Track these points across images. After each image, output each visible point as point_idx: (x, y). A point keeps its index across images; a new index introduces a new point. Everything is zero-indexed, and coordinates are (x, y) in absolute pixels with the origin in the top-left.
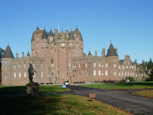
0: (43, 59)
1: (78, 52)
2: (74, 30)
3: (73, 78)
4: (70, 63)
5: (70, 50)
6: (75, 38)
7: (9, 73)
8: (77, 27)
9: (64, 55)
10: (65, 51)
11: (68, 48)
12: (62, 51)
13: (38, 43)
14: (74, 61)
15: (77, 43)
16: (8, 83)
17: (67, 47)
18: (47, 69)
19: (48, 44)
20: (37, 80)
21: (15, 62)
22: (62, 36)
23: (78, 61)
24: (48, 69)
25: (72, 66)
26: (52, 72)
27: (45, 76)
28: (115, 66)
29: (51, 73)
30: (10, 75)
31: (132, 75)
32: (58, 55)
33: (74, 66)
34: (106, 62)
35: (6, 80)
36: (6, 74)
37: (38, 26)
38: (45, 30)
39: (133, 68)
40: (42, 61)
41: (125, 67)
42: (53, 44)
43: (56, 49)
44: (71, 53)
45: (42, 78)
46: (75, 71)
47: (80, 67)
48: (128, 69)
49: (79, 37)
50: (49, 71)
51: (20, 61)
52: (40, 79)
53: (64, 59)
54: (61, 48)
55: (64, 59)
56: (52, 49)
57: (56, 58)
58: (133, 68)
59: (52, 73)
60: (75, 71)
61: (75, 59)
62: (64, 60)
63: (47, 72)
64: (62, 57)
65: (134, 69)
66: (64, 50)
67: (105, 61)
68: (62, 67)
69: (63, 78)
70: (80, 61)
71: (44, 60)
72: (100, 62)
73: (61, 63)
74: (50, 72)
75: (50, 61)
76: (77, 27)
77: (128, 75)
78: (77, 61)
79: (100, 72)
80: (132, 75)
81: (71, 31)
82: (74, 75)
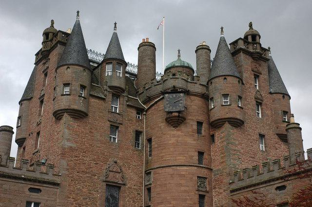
0: (50, 178)
1: (262, 147)
6: (247, 75)
8: (251, 25)
9: (181, 160)
10: (190, 140)
11: (205, 126)
12: (173, 140)
13: (45, 98)
15: (259, 104)
17: (201, 118)
19: (92, 100)
32: (147, 163)
38: (78, 28)
43: (138, 134)
49: (266, 77)
53: (181, 185)
54: (163, 125)
55: (181, 185)
56: (114, 127)
57: (132, 178)
61: (248, 182)
62: (183, 188)
66: (179, 133)
71: (58, 180)
76: (251, 25)
78: (262, 189)
81: (223, 41)
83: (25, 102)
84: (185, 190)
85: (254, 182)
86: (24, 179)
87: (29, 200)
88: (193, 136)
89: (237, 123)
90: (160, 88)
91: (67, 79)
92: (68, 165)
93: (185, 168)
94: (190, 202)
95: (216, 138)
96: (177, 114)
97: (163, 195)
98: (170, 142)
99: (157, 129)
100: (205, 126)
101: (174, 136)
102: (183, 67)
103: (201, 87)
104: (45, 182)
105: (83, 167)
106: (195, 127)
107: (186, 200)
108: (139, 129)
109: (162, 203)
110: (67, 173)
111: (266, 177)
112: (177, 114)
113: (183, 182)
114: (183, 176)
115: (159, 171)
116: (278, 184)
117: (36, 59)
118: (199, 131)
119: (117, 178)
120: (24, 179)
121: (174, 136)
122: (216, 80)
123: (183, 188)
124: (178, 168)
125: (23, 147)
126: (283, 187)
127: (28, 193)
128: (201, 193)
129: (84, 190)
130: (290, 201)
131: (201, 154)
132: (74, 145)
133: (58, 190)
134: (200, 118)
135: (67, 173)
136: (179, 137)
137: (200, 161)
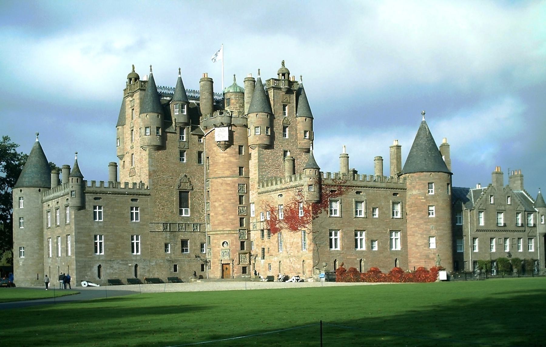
2: (269, 73)
7: (35, 242)
8: (283, 63)
9: (227, 173)
10: (233, 160)
12: (222, 160)
14: (264, 197)
18: (161, 228)
20: (116, 266)
22: (233, 101)
24: (165, 229)
26: (182, 237)
27: (149, 252)
29: (179, 240)
31: (526, 247)
34: (395, 198)
35: (23, 265)
37: (134, 68)
39: (532, 222)
40: (135, 197)
41: (491, 219)
42: (188, 134)
45: (136, 261)
48: (505, 225)
52: (127, 264)
58: (532, 222)
59: (184, 243)
62: (228, 192)
63: (161, 239)
64: (220, 180)
65: (535, 226)
66: (226, 155)
67: (390, 192)
68: (220, 217)
70: (281, 195)
72: (363, 196)
73: (217, 204)
74: (174, 236)
75: (175, 198)
76: (283, 63)
77: (507, 250)
79: (363, 237)
80: (526, 247)
84: (230, 194)
86: (128, 194)
87: (132, 206)
88: (235, 156)
92: (153, 182)
94: (232, 201)
97: (216, 197)
98: (220, 161)
99: (212, 151)
102: (236, 92)
103: (241, 119)
104: (140, 195)
105: (163, 182)
106: (237, 150)
107: (230, 200)
108: (201, 150)
109: (216, 201)
110: (153, 187)
114: (229, 184)
116: (279, 193)
117: (125, 94)
118: (240, 152)
119: (187, 187)
120: (128, 194)
123: (228, 192)
124: (225, 179)
125: (123, 160)
127: (131, 202)
128: (240, 194)
129: (165, 196)
130: (283, 203)
131: (241, 168)
132: (156, 169)
133: (148, 198)
134: (241, 143)
135: (153, 187)
136: (226, 157)
137: (240, 173)
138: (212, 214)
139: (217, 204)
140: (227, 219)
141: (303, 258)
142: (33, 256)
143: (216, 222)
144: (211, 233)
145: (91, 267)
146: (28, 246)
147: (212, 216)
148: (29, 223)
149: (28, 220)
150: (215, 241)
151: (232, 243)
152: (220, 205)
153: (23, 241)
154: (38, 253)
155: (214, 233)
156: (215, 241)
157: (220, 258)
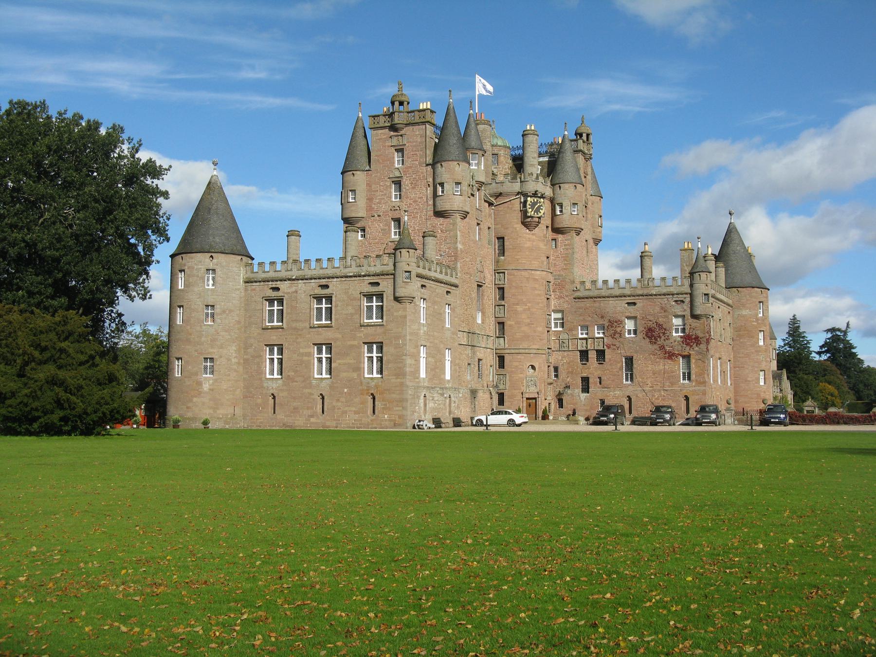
3: (584, 396)
4: (559, 315)
5: (560, 237)
9: (535, 264)
10: (542, 245)
12: (528, 244)
13: (406, 182)
16: (221, 412)
21: (278, 284)
23: (622, 304)
25: (571, 330)
28: (761, 343)
30: (233, 360)
32: (497, 262)
33: (585, 327)
36: (214, 352)
44: (568, 260)
46: (592, 355)
47: (627, 336)
50: (469, 350)
51: (323, 282)
52: (442, 395)
53: (535, 289)
55: (535, 289)
60: (592, 355)
62: (537, 292)
66: (534, 237)
68: (525, 329)
69: (532, 392)
73: (519, 308)
78: (612, 302)
82: (586, 381)
83: (358, 172)
85: (604, 294)
89: (578, 231)
90: (517, 187)
91: (459, 178)
93: (538, 273)
95: (559, 244)
96: (537, 220)
100: (550, 229)
101: (529, 240)
107: (538, 303)
109: (517, 304)
111: (617, 292)
112: (537, 220)
113: (537, 286)
115: (516, 273)
121: (529, 240)
122: (566, 186)
123: (537, 292)
126: (634, 304)
136: (533, 241)
138: (508, 323)
139: (519, 308)
140: (535, 331)
141: (685, 392)
142: (229, 375)
143: (518, 335)
144: (508, 351)
145: (418, 397)
146: (221, 357)
147: (510, 326)
148: (224, 316)
149: (224, 312)
150: (515, 364)
151: (540, 367)
152: (525, 310)
153: (212, 347)
154: (236, 371)
155: (513, 351)
156: (515, 364)
157: (524, 389)
